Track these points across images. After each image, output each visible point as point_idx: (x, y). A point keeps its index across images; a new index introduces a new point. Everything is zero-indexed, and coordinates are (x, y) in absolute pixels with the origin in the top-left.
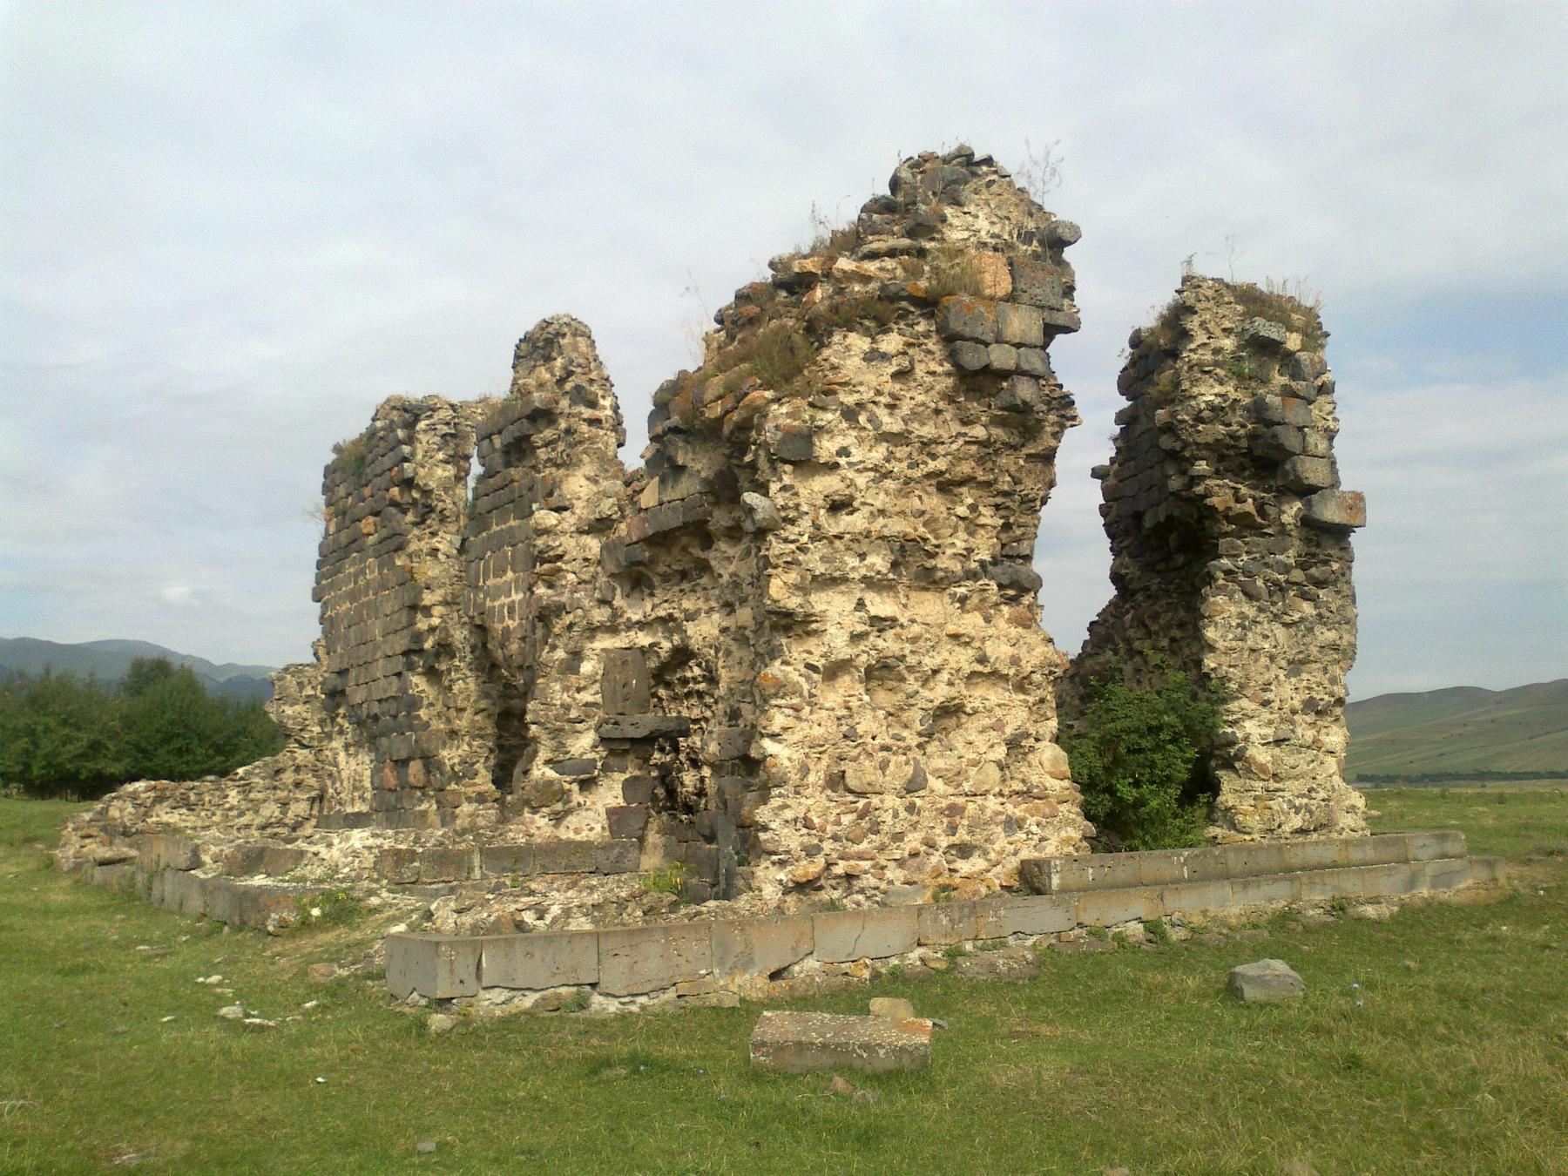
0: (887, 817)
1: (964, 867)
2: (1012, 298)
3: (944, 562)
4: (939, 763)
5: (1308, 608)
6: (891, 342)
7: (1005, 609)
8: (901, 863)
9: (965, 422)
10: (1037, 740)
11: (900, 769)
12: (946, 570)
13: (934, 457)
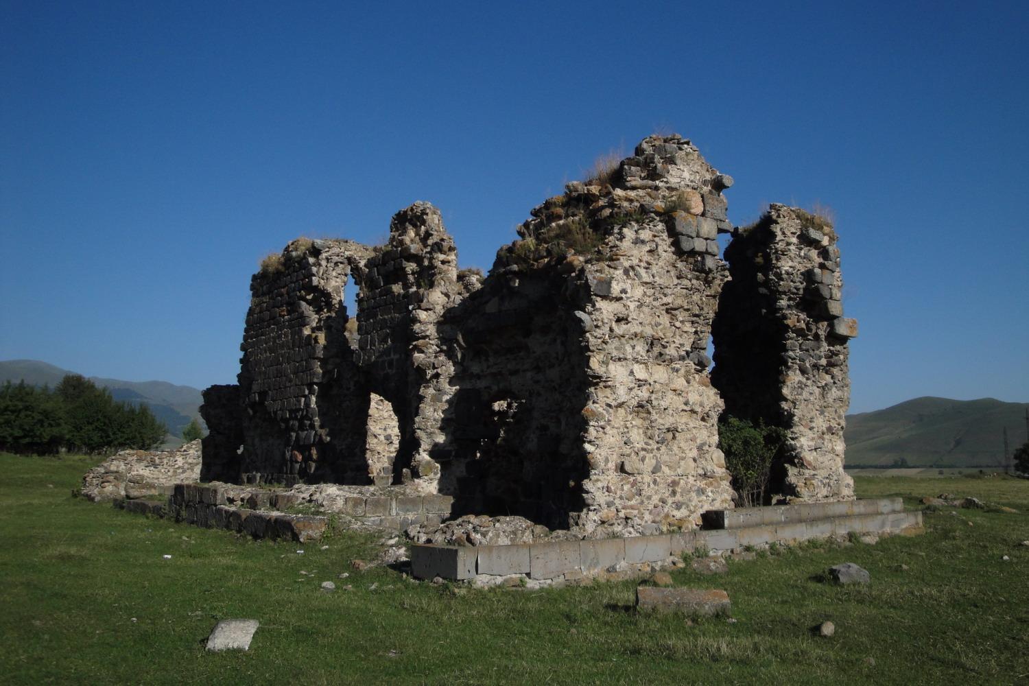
2: (703, 215)
6: (645, 234)
11: (650, 462)
13: (665, 295)
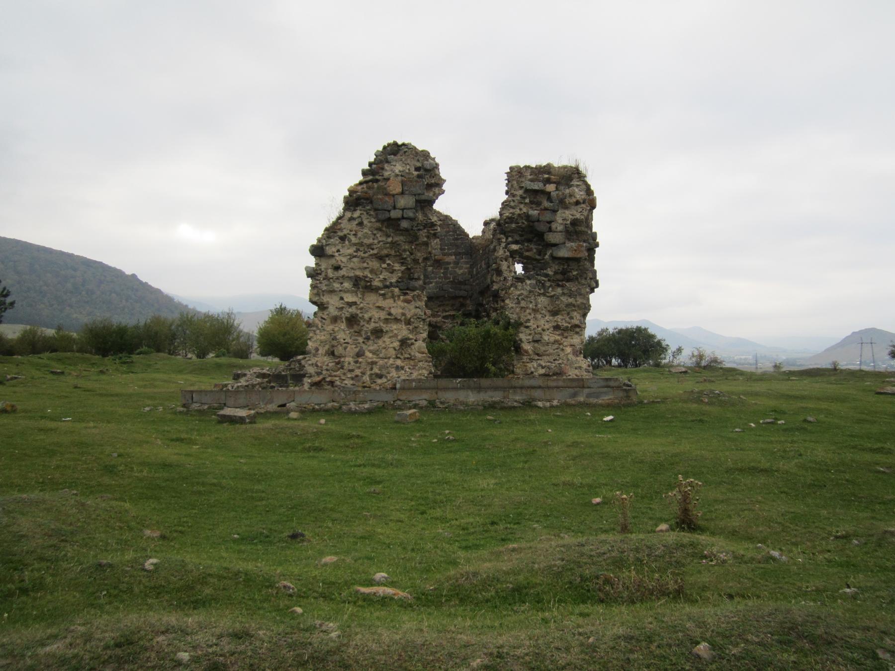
0: (346, 364)
1: (379, 381)
2: (402, 193)
3: (376, 283)
4: (371, 348)
5: (559, 290)
6: (357, 214)
7: (402, 297)
8: (352, 379)
9: (388, 236)
11: (352, 350)
13: (373, 249)
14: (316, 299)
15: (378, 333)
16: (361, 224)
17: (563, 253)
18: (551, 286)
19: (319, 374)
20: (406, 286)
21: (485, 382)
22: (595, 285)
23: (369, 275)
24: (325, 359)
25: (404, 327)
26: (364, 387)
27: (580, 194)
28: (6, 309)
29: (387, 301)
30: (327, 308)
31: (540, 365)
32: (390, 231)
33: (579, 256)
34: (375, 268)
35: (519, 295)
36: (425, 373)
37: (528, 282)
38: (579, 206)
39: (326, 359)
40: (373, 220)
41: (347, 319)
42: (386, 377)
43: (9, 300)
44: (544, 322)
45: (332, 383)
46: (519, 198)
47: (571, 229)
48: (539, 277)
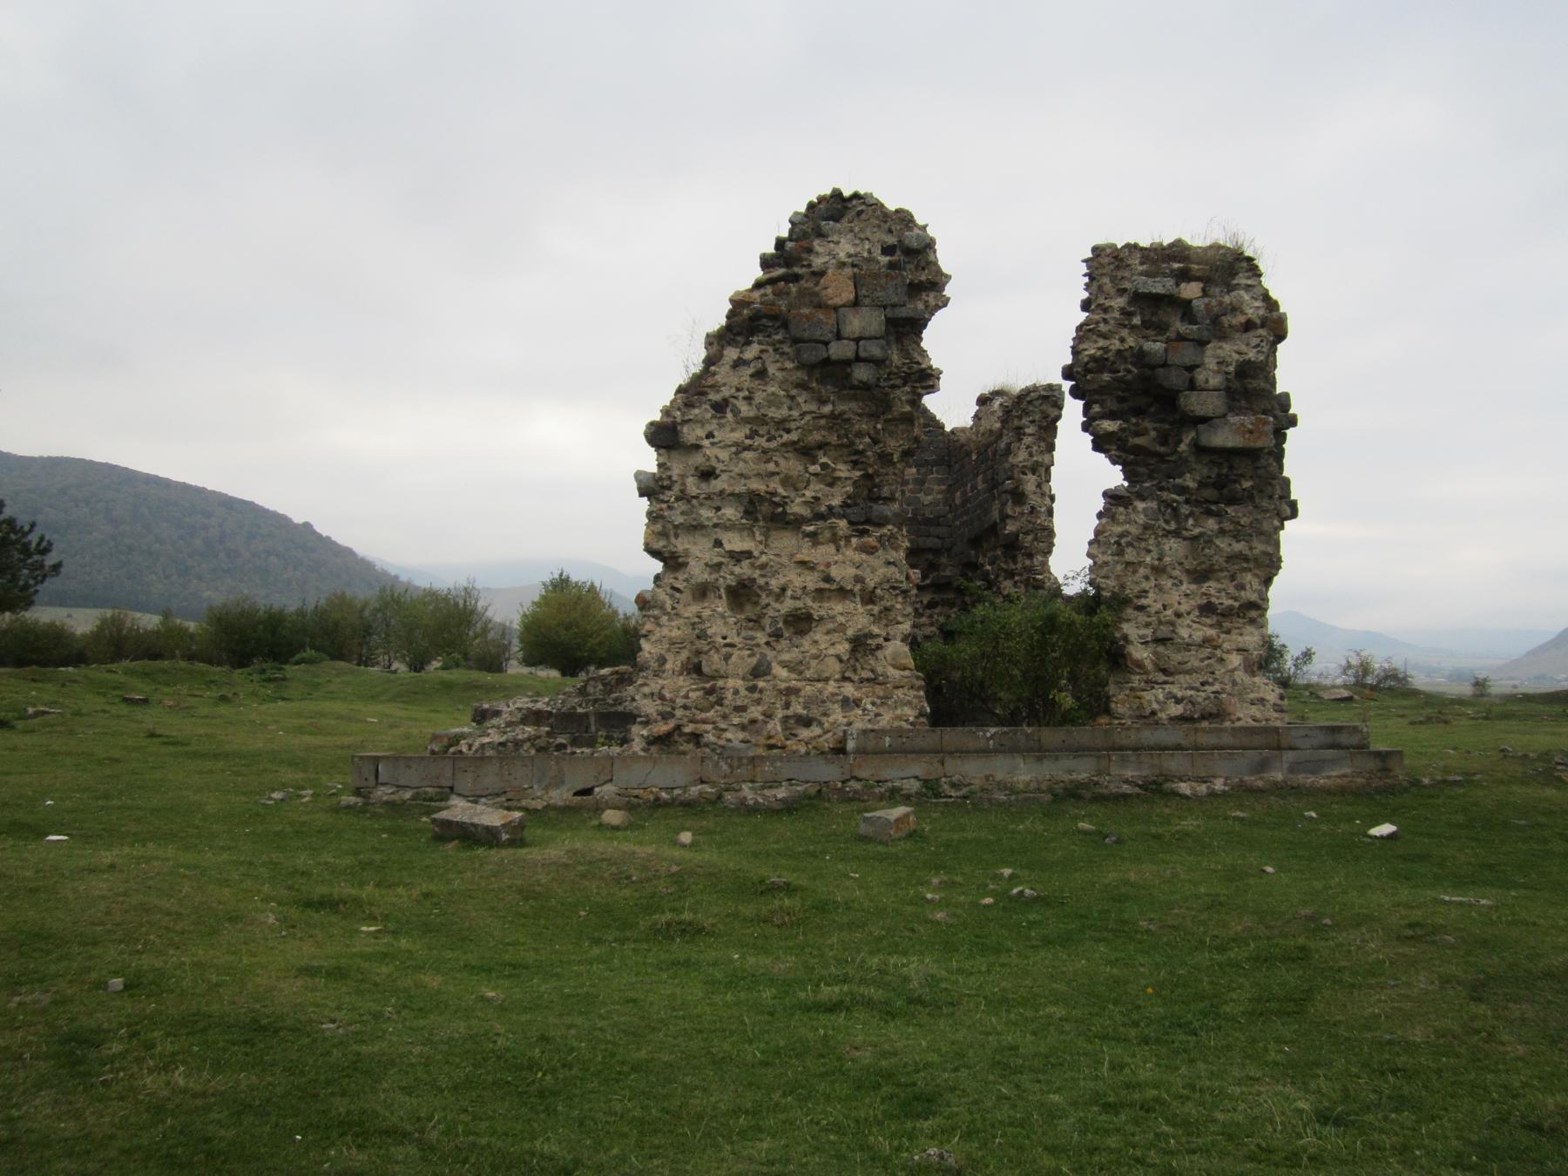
0: (729, 695)
1: (805, 733)
2: (856, 303)
3: (797, 508)
4: (786, 657)
5: (1212, 524)
6: (751, 352)
7: (854, 541)
8: (743, 727)
9: (822, 402)
10: (887, 640)
11: (742, 661)
12: (794, 514)
13: (788, 431)
14: (659, 544)
15: (801, 622)
16: (761, 374)
17: (1223, 438)
18: (1191, 514)
19: (665, 716)
20: (863, 514)
21: (1051, 736)
22: (1289, 511)
23: (780, 490)
24: (681, 681)
25: (860, 609)
26: (771, 747)
27: (1254, 309)
28: (44, 577)
29: (822, 549)
30: (685, 565)
31: (1171, 696)
32: (828, 390)
33: (1259, 444)
34: (794, 473)
35: (1121, 536)
36: (910, 713)
37: (1140, 505)
38: (1251, 334)
39: (684, 683)
40: (789, 365)
41: (729, 589)
42: (820, 724)
43: (50, 560)
44: (1178, 597)
45: (696, 738)
46: (1117, 314)
47: (1236, 385)
48: (1165, 495)
